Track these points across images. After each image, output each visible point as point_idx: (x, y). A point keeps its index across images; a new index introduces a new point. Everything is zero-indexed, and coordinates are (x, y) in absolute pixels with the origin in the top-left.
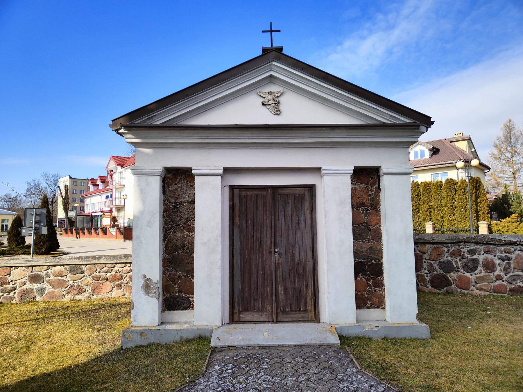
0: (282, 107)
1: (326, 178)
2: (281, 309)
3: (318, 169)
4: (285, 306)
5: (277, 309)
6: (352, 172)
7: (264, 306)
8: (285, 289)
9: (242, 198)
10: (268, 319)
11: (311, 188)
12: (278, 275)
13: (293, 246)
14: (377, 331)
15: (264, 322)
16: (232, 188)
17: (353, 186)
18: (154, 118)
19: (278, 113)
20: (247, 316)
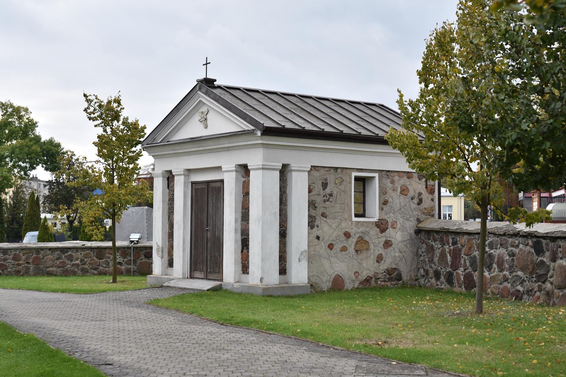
0: (209, 122)
1: (225, 174)
2: (209, 270)
3: (219, 168)
4: (210, 269)
5: (207, 270)
6: (234, 169)
7: (203, 269)
8: (211, 257)
9: (197, 190)
10: (204, 276)
11: (222, 181)
12: (209, 246)
13: (215, 225)
14: (239, 288)
15: (202, 279)
16: (193, 183)
17: (244, 179)
18: (156, 139)
19: (206, 127)
20: (197, 274)
